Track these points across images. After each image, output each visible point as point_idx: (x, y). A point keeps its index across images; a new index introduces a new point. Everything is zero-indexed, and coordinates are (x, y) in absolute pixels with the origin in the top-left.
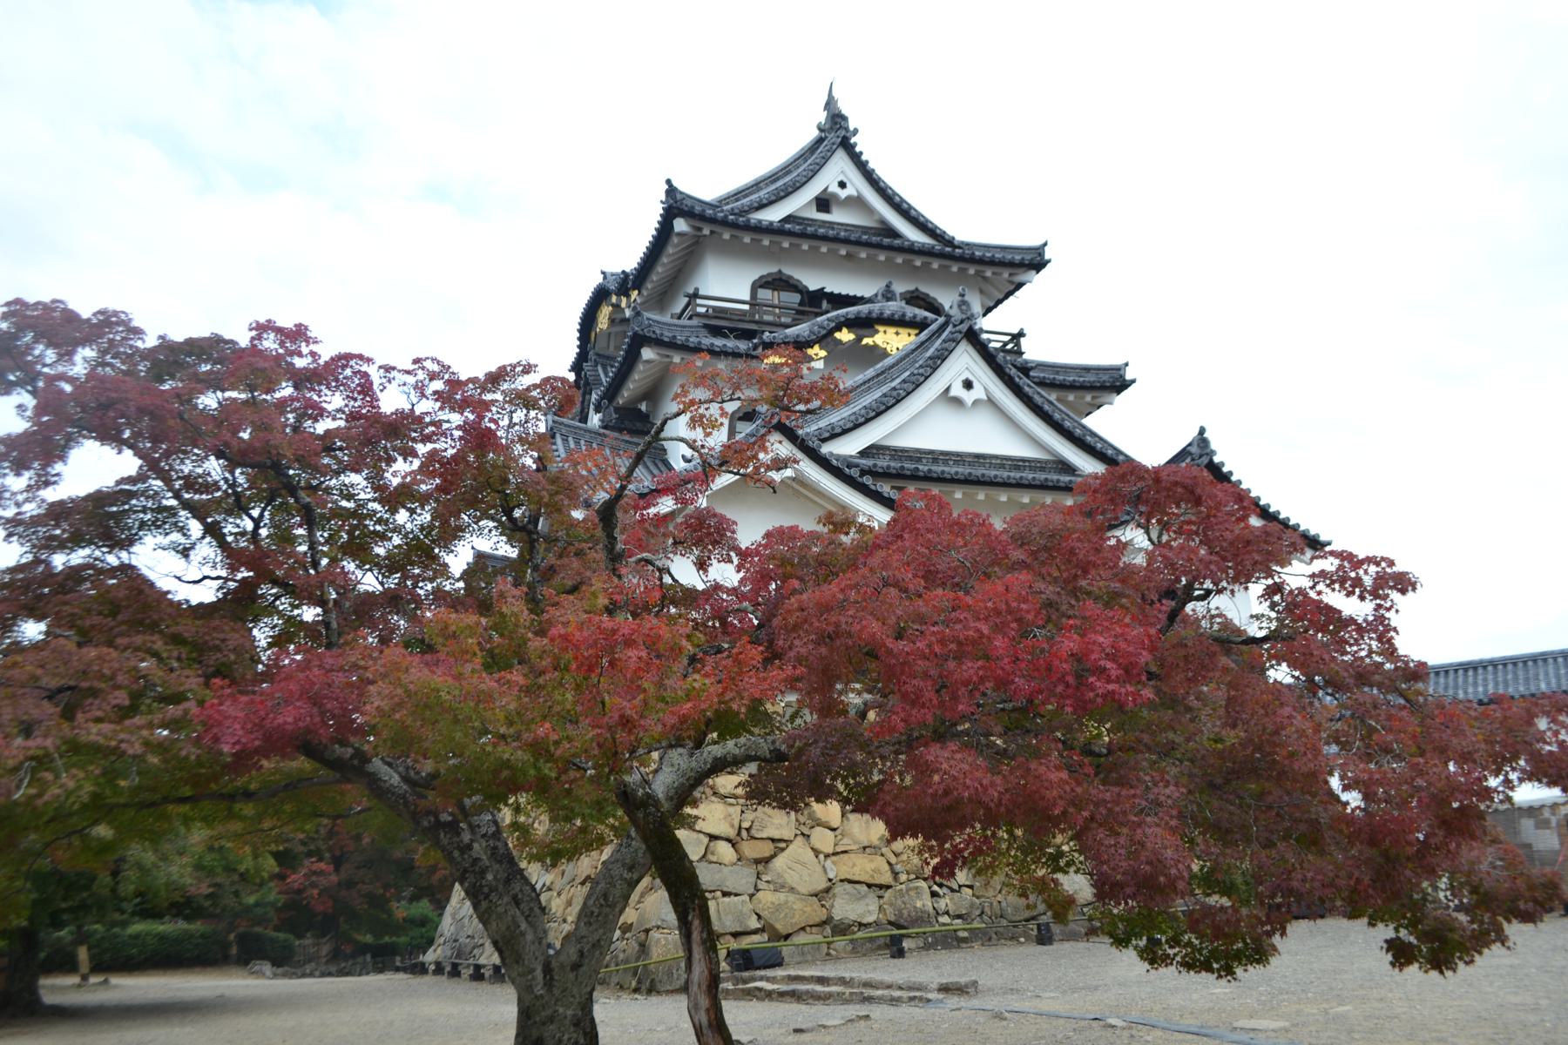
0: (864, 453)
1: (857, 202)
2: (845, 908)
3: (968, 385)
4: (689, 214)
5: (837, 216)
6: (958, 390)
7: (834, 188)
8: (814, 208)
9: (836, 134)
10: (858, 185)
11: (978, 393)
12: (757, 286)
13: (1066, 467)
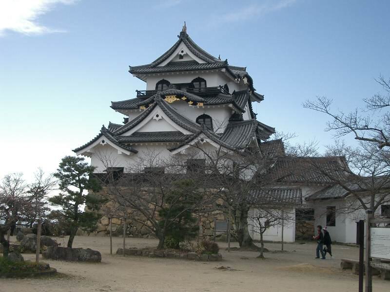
0: (134, 135)
1: (187, 55)
2: (109, 228)
3: (157, 116)
5: (185, 59)
6: (155, 117)
8: (178, 58)
9: (184, 37)
10: (186, 51)
11: (160, 117)
12: (157, 84)
13: (180, 133)
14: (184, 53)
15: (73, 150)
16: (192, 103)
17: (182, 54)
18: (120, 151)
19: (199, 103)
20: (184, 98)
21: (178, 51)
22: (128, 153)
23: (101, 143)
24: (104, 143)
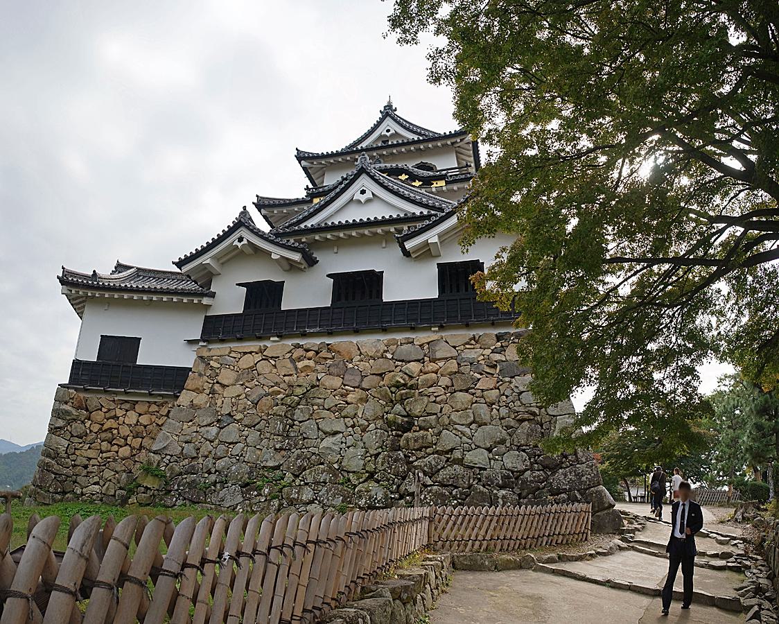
4: (305, 158)
7: (385, 133)
9: (388, 112)
10: (395, 128)
14: (392, 132)
15: (173, 263)
16: (421, 183)
17: (388, 134)
18: (277, 252)
19: (435, 183)
20: (404, 177)
21: (381, 130)
22: (296, 257)
23: (236, 243)
24: (242, 243)
